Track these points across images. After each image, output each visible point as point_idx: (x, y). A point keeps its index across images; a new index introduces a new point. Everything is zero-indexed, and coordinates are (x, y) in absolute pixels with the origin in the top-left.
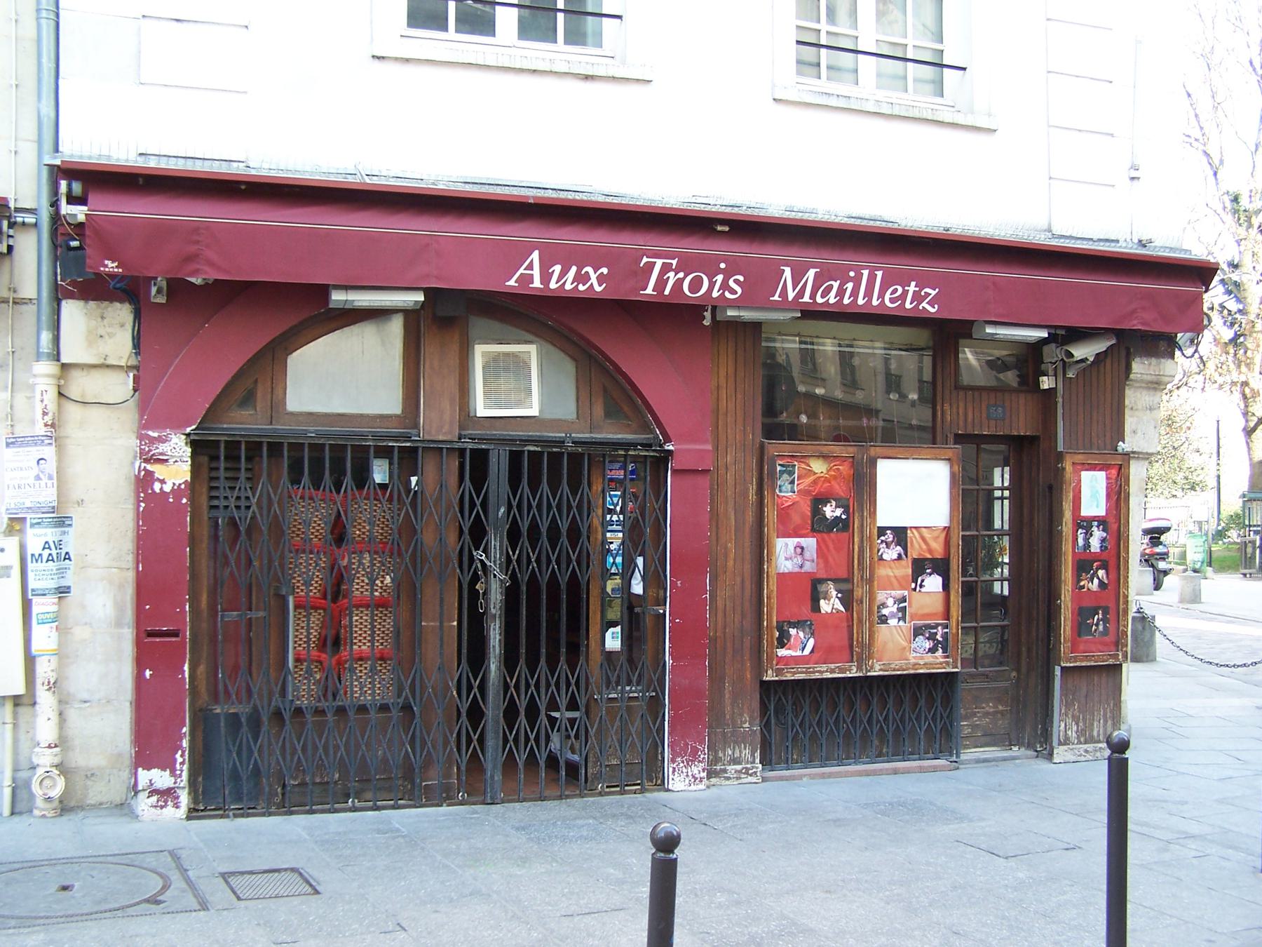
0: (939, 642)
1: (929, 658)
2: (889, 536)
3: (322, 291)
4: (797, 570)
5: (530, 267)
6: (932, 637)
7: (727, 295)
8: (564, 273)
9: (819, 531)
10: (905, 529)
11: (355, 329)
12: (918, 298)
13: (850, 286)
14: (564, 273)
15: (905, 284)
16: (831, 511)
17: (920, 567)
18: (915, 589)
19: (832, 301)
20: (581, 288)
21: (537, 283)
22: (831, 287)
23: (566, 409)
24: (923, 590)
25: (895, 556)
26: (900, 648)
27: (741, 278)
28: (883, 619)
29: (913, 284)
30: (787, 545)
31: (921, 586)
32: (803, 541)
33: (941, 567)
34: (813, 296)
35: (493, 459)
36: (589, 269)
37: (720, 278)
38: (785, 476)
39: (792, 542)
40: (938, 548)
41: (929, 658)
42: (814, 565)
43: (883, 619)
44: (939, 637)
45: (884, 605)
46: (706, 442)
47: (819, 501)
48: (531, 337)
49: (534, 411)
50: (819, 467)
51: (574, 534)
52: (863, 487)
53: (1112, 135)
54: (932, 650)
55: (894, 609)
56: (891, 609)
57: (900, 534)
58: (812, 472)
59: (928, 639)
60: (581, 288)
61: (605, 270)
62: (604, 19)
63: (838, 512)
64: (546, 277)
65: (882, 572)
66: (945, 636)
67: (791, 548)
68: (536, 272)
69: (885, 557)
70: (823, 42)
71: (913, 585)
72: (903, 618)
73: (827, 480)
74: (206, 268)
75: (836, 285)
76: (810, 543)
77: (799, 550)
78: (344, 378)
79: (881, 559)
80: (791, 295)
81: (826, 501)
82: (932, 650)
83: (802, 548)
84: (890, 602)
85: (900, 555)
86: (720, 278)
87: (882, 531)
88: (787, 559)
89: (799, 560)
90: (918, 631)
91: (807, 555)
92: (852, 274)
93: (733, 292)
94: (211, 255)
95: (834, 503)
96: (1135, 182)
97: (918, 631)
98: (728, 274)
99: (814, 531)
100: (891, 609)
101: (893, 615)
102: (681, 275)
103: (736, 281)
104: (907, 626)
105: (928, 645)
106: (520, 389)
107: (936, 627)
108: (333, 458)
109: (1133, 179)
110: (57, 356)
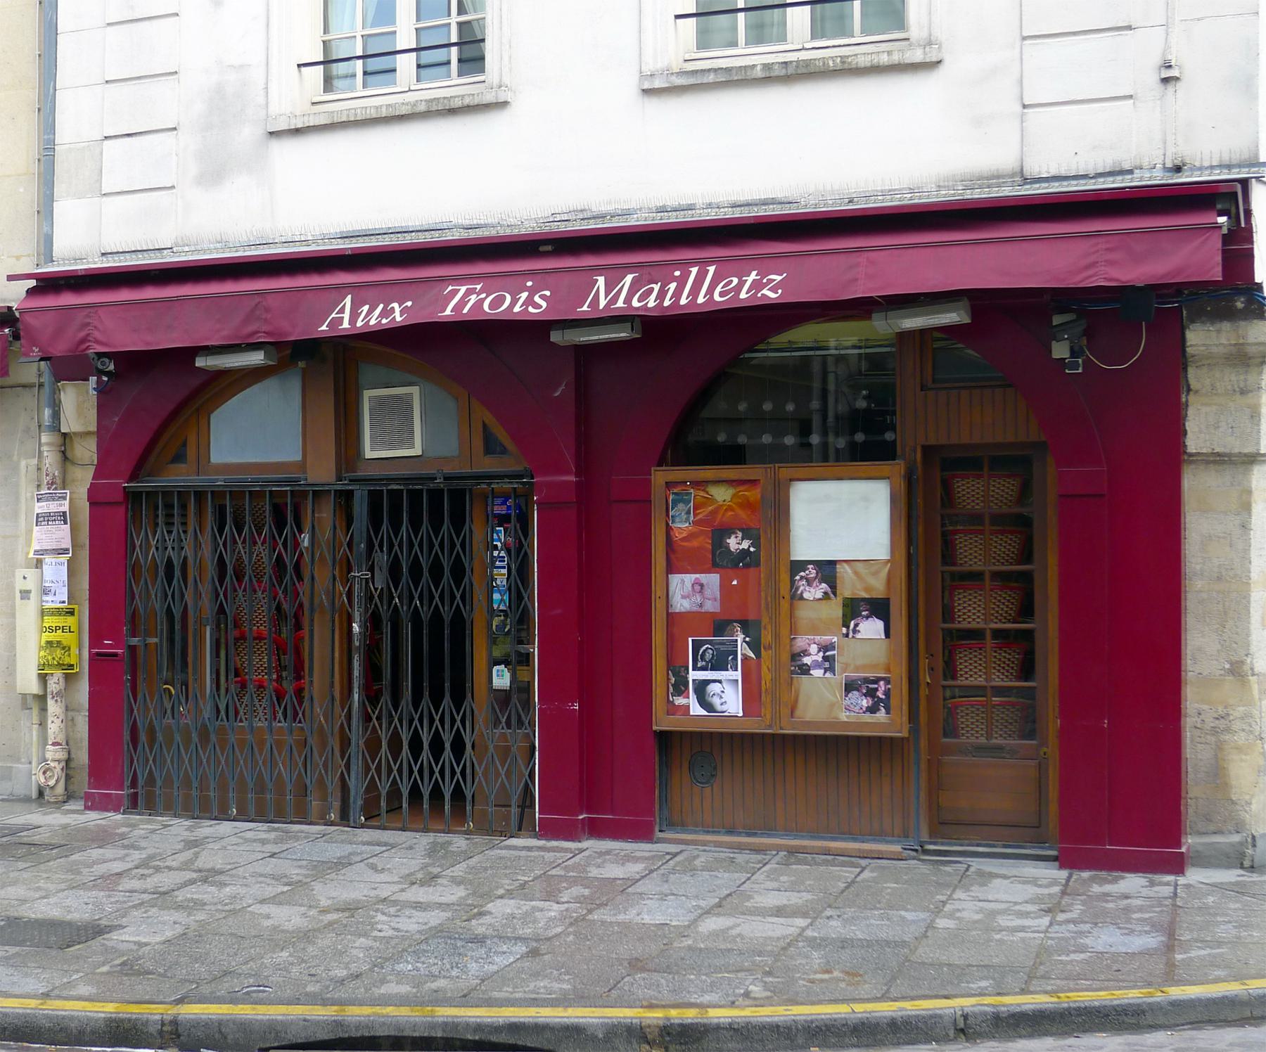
0: (881, 700)
1: (868, 718)
2: (812, 572)
3: (186, 355)
4: (695, 609)
5: (342, 311)
6: (871, 693)
7: (531, 309)
8: (370, 312)
9: (723, 567)
10: (833, 563)
11: (255, 389)
12: (757, 285)
13: (673, 286)
14: (370, 312)
15: (741, 275)
16: (735, 543)
17: (853, 610)
18: (847, 635)
19: (651, 304)
20: (384, 321)
21: (346, 325)
22: (652, 289)
23: (449, 446)
24: (858, 636)
25: (819, 595)
26: (825, 702)
27: (548, 293)
28: (805, 670)
29: (754, 273)
30: (683, 581)
31: (855, 631)
32: (703, 577)
33: (879, 608)
34: (628, 300)
35: (357, 495)
36: (395, 305)
37: (524, 295)
38: (681, 506)
39: (689, 578)
40: (877, 586)
41: (868, 718)
42: (718, 604)
43: (805, 670)
44: (880, 694)
45: (806, 653)
46: (568, 473)
47: (721, 533)
48: (414, 379)
49: (417, 451)
50: (722, 494)
51: (459, 572)
52: (776, 517)
53: (1129, 28)
54: (872, 710)
55: (819, 658)
56: (814, 656)
57: (827, 570)
58: (711, 500)
59: (865, 695)
60: (384, 321)
61: (409, 304)
62: (789, 10)
63: (745, 545)
64: (354, 316)
65: (805, 614)
66: (887, 693)
67: (688, 585)
68: (346, 316)
69: (806, 595)
70: (360, 63)
71: (844, 630)
72: (831, 669)
73: (730, 508)
74: (95, 346)
75: (656, 287)
76: (712, 580)
77: (697, 588)
78: (256, 435)
79: (801, 598)
80: (603, 303)
81: (727, 531)
82: (872, 710)
83: (702, 585)
84: (813, 649)
85: (825, 593)
86: (524, 295)
87: (800, 566)
88: (684, 597)
89: (698, 599)
90: (850, 687)
91: (708, 592)
92: (677, 273)
93: (538, 306)
94: (97, 334)
95: (740, 534)
96: (1170, 88)
97: (850, 687)
98: (533, 292)
99: (714, 567)
100: (814, 656)
101: (817, 665)
102: (483, 296)
103: (542, 297)
104: (839, 678)
105: (865, 702)
106: (407, 432)
107: (876, 681)
108: (273, 506)
109: (1166, 81)
110: (55, 427)
